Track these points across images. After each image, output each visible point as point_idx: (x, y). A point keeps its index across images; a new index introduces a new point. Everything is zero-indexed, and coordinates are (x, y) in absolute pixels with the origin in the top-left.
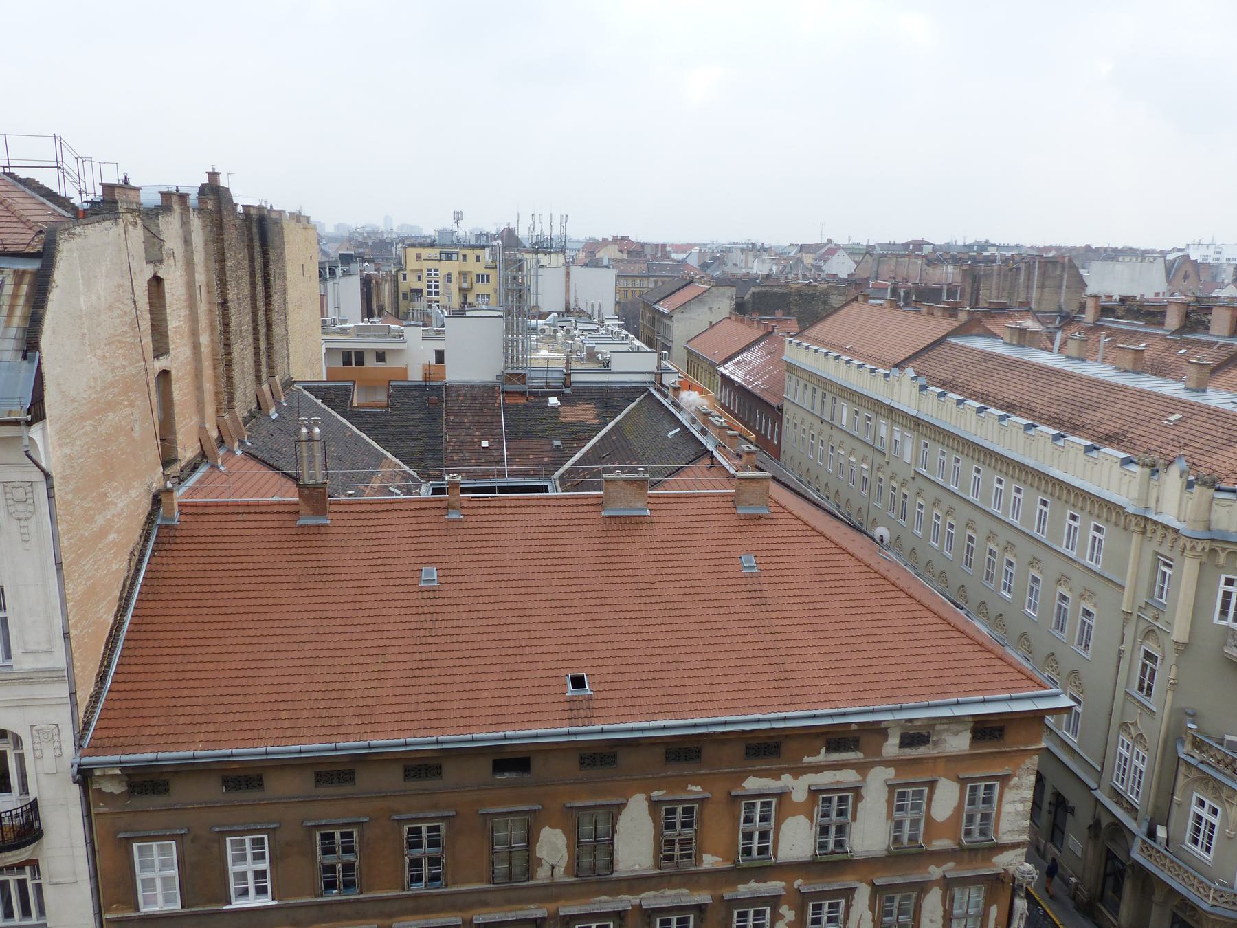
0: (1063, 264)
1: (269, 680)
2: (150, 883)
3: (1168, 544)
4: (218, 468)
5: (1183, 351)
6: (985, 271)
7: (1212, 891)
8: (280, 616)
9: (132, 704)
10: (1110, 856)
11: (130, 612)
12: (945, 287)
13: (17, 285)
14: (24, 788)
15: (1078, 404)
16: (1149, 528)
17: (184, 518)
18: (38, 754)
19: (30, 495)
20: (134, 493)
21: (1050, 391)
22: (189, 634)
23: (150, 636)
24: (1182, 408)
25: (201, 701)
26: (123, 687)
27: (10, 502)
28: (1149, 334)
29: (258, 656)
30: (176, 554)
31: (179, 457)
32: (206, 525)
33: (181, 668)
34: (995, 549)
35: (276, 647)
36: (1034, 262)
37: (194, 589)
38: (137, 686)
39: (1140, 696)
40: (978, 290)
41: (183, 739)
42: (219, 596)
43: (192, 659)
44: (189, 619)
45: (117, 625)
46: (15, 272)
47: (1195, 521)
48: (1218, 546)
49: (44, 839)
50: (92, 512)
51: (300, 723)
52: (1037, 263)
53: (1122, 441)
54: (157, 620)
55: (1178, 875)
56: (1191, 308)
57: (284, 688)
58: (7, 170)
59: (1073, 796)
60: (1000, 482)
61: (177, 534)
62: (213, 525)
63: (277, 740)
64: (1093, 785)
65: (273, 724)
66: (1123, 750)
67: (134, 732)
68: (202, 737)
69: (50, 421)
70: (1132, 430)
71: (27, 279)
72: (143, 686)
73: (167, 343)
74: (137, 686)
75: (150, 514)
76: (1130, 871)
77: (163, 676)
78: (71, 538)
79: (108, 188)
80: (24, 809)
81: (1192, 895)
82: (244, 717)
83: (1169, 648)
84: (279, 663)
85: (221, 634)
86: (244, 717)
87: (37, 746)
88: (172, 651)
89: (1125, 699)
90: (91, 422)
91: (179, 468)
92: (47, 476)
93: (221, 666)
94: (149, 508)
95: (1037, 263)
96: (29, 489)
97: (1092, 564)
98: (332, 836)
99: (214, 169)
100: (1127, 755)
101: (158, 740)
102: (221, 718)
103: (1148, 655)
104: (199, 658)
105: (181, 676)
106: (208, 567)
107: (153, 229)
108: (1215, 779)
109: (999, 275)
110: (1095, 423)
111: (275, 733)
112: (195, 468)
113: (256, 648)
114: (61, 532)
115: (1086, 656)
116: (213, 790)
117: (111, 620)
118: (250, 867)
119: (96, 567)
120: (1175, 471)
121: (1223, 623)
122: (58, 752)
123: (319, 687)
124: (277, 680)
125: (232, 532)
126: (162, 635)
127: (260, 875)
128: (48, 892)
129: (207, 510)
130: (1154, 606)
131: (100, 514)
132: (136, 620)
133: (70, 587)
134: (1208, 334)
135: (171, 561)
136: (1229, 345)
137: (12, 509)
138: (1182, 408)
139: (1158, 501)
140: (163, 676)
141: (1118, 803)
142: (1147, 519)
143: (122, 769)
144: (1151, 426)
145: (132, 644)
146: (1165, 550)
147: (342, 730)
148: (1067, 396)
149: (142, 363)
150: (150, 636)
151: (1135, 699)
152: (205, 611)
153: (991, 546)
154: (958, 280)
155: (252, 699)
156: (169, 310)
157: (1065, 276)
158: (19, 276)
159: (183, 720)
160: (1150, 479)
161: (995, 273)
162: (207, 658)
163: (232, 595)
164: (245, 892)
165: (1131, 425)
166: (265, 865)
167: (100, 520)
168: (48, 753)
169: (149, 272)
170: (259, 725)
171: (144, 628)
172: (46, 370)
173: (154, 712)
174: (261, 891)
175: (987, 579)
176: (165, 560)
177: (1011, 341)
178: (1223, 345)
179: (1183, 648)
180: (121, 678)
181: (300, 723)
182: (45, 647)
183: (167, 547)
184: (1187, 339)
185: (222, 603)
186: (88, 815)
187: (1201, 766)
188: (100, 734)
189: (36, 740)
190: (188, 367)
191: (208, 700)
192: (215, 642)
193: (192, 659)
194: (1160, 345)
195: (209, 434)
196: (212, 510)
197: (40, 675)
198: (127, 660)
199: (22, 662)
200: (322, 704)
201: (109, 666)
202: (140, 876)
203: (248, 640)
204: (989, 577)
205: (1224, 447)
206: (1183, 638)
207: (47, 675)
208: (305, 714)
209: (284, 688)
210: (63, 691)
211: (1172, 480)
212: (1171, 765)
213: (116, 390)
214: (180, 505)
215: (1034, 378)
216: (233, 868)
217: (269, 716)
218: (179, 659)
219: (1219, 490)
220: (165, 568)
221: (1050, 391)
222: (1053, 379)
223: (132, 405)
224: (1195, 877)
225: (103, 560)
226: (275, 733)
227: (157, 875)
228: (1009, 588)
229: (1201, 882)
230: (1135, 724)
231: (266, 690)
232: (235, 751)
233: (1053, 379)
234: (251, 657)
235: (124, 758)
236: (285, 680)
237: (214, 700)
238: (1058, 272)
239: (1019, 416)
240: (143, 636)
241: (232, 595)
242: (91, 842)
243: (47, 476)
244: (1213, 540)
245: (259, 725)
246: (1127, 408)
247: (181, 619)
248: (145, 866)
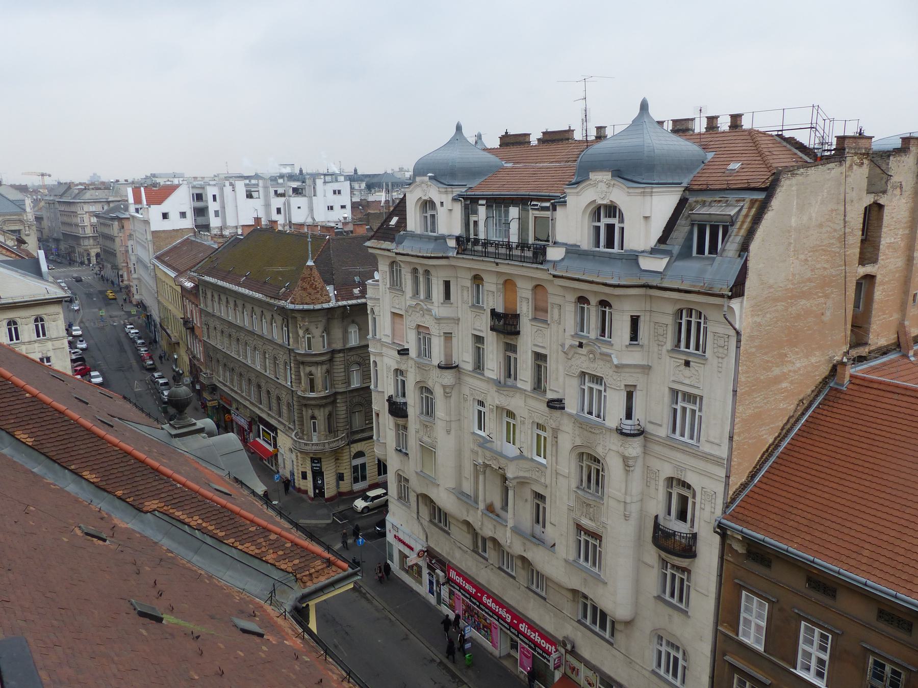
1: (864, 523)
2: (747, 622)
4: (908, 357)
8: (897, 480)
9: (765, 500)
11: (788, 440)
13: (750, 208)
14: (692, 526)
17: (851, 386)
18: (703, 506)
19: (726, 343)
20: (813, 360)
22: (819, 468)
23: (794, 460)
25: (809, 516)
26: (764, 486)
27: (715, 345)
29: (864, 502)
30: (835, 410)
31: (870, 342)
32: (866, 396)
33: (805, 489)
35: (881, 501)
37: (837, 438)
38: (772, 489)
41: (786, 536)
42: (853, 449)
43: (816, 486)
44: (824, 458)
45: (776, 445)
46: (752, 200)
49: (696, 560)
50: (770, 364)
51: (876, 564)
54: (803, 451)
57: (875, 534)
58: (780, 133)
61: (842, 396)
62: (871, 397)
63: (851, 568)
65: (854, 556)
67: (759, 517)
68: (799, 540)
69: (748, 298)
71: (756, 205)
72: (776, 491)
73: (877, 255)
74: (772, 489)
75: (826, 378)
77: (790, 489)
78: (748, 377)
79: (841, 139)
80: (688, 535)
82: (834, 540)
84: (879, 514)
85: (844, 476)
86: (834, 540)
87: (703, 501)
88: (804, 475)
90: (783, 304)
91: (867, 350)
92: (738, 333)
93: (834, 498)
94: (827, 373)
96: (726, 340)
98: (883, 666)
99: (570, 127)
101: (771, 529)
102: (817, 534)
104: (820, 487)
105: (803, 494)
106: (854, 426)
107: (884, 167)
111: (853, 563)
112: (885, 353)
113: (866, 496)
114: (740, 371)
116: (799, 583)
117: (771, 441)
118: (816, 653)
119: (765, 401)
122: (713, 510)
123: (904, 545)
124: (871, 526)
125: (884, 406)
126: (802, 462)
127: (821, 662)
128: (693, 594)
129: (871, 385)
131: (777, 367)
132: (789, 447)
133: (740, 409)
135: (829, 414)
137: (716, 350)
140: (790, 489)
143: (743, 537)
145: (780, 461)
147: (909, 586)
149: (844, 268)
150: (794, 460)
152: (839, 456)
155: (846, 531)
156: (884, 230)
158: (753, 202)
159: (791, 523)
162: (826, 489)
163: (864, 452)
164: (808, 669)
166: (826, 657)
167: (777, 371)
168: (708, 508)
169: (869, 200)
170: (843, 551)
171: (792, 453)
172: (750, 264)
173: (776, 510)
174: (820, 675)
176: (825, 413)
180: (765, 480)
181: (876, 564)
182: (717, 441)
183: (831, 404)
185: (853, 455)
186: (722, 558)
188: (738, 509)
189: (703, 497)
190: (897, 275)
191: (814, 518)
192: (837, 480)
193: (816, 486)
195: (907, 329)
196: (876, 386)
197: (712, 458)
198: (773, 471)
199: (706, 448)
200: (901, 559)
201: (759, 470)
202: (743, 615)
203: (862, 488)
207: (715, 459)
208: (882, 559)
209: (875, 534)
210: (722, 473)
213: (813, 284)
214: (852, 376)
216: (802, 646)
217: (855, 548)
218: (807, 483)
220: (822, 418)
223: (827, 296)
225: (773, 398)
226: (853, 563)
227: (754, 621)
231: (860, 528)
232: (816, 560)
234: (859, 501)
235: (745, 530)
236: (879, 528)
237: (817, 519)
240: (790, 459)
241: (864, 452)
242: (720, 576)
243: (738, 333)
245: (843, 551)
247: (819, 456)
248: (748, 610)
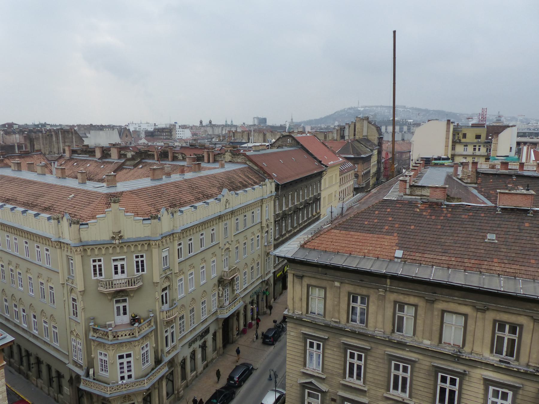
0: (72, 132)
3: (69, 251)
5: (103, 166)
6: (35, 136)
7: (109, 388)
10: (79, 390)
12: (16, 144)
15: (37, 195)
16: (62, 245)
21: (26, 191)
24: (75, 192)
28: (90, 160)
34: (13, 269)
36: (58, 132)
39: (74, 317)
40: (34, 145)
47: (75, 239)
48: (86, 247)
52: (60, 132)
53: (51, 209)
55: (97, 387)
56: (104, 149)
59: (62, 371)
60: (8, 236)
64: (67, 362)
66: (73, 343)
70: (56, 204)
76: (84, 393)
81: (103, 394)
83: (79, 293)
89: (70, 321)
95: (60, 132)
97: (47, 266)
100: (75, 344)
103: (74, 300)
108: (103, 343)
109: (43, 138)
110: (42, 203)
115: (54, 307)
120: (65, 219)
121: (96, 278)
130: (71, 278)
134: (111, 158)
136: (118, 162)
138: (75, 192)
139: (62, 234)
141: (76, 366)
142: (60, 242)
144: (63, 201)
146: (69, 254)
148: (33, 192)
151: (73, 320)
153: (11, 267)
154: (22, 141)
157: (74, 137)
160: (58, 224)
161: (41, 137)
165: (56, 202)
175: (12, 283)
177: (15, 169)
178: (116, 163)
179: (83, 293)
184: (104, 161)
187: (98, 339)
194: (95, 164)
204: (13, 282)
205: (87, 206)
206: (83, 289)
211: (65, 223)
212: (88, 342)
215: (20, 185)
219: (82, 224)
221: (26, 191)
222: (28, 185)
224: (102, 385)
228: (22, 285)
229: (104, 387)
230: (75, 330)
233: (28, 185)
238: (70, 136)
239: (11, 204)
244: (83, 246)
246: (55, 194)
